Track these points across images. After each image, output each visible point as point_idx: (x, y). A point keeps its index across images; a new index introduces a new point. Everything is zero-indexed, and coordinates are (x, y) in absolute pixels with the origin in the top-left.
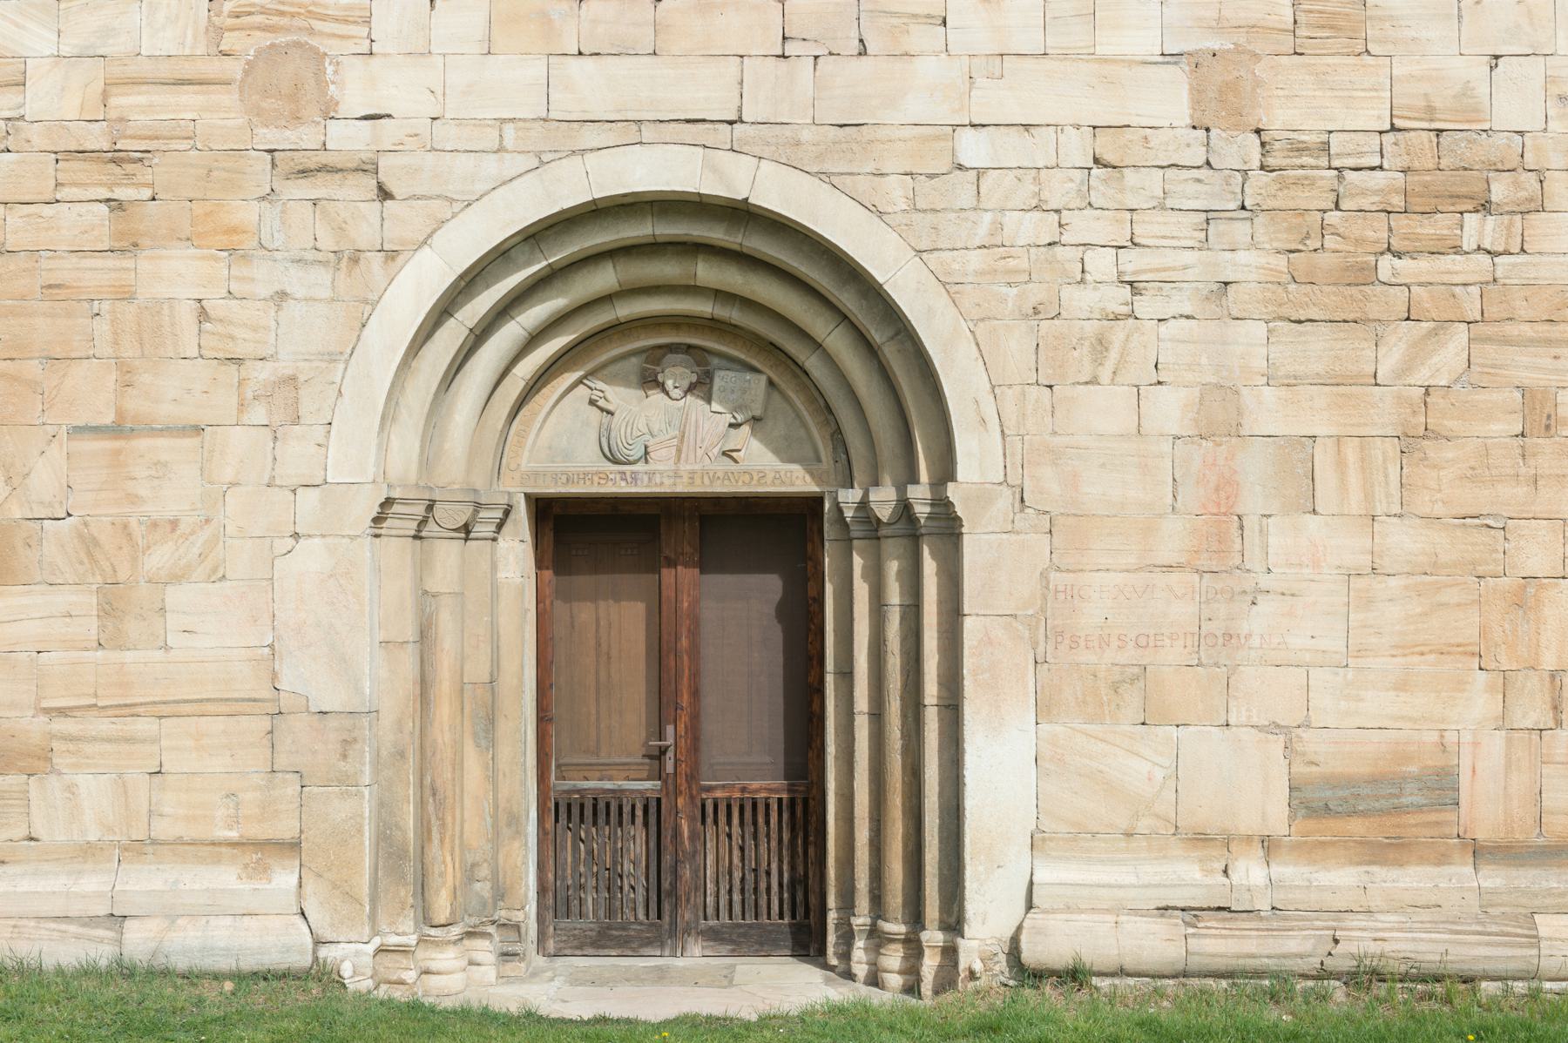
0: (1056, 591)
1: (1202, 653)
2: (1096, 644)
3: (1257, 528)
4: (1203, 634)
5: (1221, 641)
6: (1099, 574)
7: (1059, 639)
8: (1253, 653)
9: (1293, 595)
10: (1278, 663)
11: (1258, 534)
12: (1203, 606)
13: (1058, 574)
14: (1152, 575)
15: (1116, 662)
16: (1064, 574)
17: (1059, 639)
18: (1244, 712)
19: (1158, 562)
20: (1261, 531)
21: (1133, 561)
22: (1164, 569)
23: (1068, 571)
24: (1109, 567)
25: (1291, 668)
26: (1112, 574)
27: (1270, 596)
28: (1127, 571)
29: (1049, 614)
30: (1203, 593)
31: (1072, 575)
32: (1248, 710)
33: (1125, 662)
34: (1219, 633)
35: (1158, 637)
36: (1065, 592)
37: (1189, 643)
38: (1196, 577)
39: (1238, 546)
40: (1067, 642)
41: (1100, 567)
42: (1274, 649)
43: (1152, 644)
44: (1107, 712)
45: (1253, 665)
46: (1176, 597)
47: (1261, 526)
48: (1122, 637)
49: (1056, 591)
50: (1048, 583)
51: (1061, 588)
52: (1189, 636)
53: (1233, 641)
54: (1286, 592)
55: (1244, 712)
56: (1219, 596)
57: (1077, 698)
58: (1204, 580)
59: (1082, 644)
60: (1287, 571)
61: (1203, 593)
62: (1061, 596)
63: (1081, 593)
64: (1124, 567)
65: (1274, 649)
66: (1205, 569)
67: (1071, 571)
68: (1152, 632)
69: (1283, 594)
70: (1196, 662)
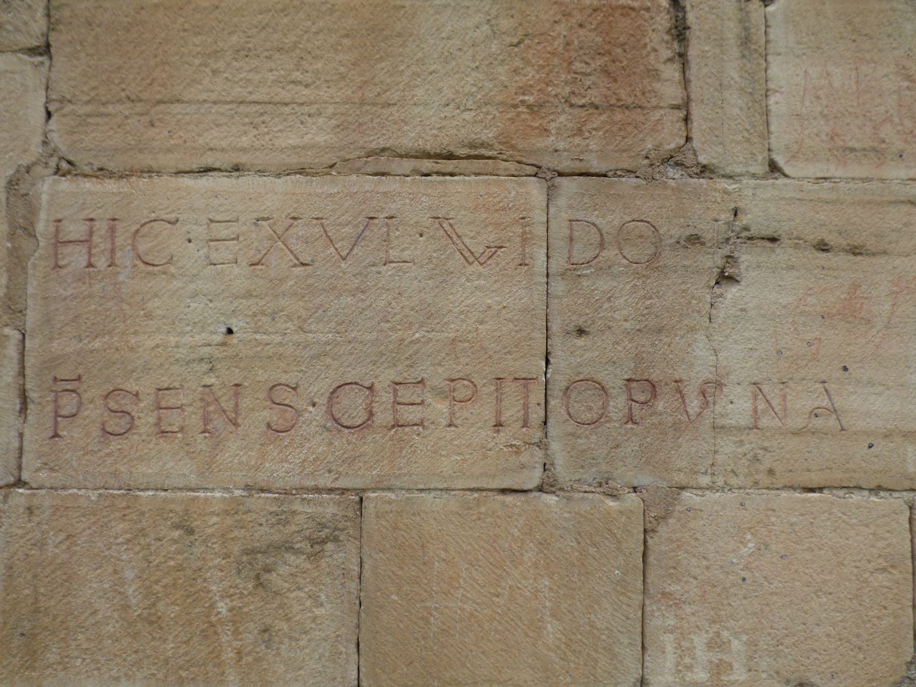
0: (59, 242)
1: (555, 447)
2: (194, 421)
3: (732, 30)
4: (559, 382)
5: (618, 404)
6: (206, 182)
7: (68, 404)
8: (727, 447)
9: (855, 251)
10: (815, 479)
11: (735, 52)
12: (559, 287)
13: (65, 185)
14: (389, 184)
15: (262, 478)
16: (88, 185)
17: (68, 404)
18: (701, 653)
19: (408, 140)
20: (746, 41)
21: (321, 139)
22: (427, 165)
23: (102, 173)
24: (243, 159)
25: (856, 498)
26: (248, 183)
27: (781, 255)
28: (302, 171)
29: (32, 318)
30: (559, 243)
31: (111, 186)
32: (716, 644)
33: (294, 481)
34: (613, 379)
35: (406, 394)
36: (87, 241)
37: (512, 413)
38: (535, 190)
39: (671, 92)
40: (93, 412)
41: (209, 160)
42: (796, 433)
43: (383, 417)
44: (229, 655)
45: (727, 487)
46: (470, 258)
47: (744, 21)
48: (282, 395)
49: (59, 242)
50: (32, 210)
51: (74, 230)
52: (511, 389)
53: (660, 405)
54: (831, 239)
55: (701, 653)
56: (610, 253)
57: (126, 607)
58: (561, 201)
59: (146, 421)
60: (833, 170)
61: (559, 243)
62: (76, 258)
63: (142, 247)
64: (294, 160)
65: (796, 433)
66: (565, 164)
67: (111, 175)
68: (385, 377)
69: (823, 247)
70: (534, 477)
